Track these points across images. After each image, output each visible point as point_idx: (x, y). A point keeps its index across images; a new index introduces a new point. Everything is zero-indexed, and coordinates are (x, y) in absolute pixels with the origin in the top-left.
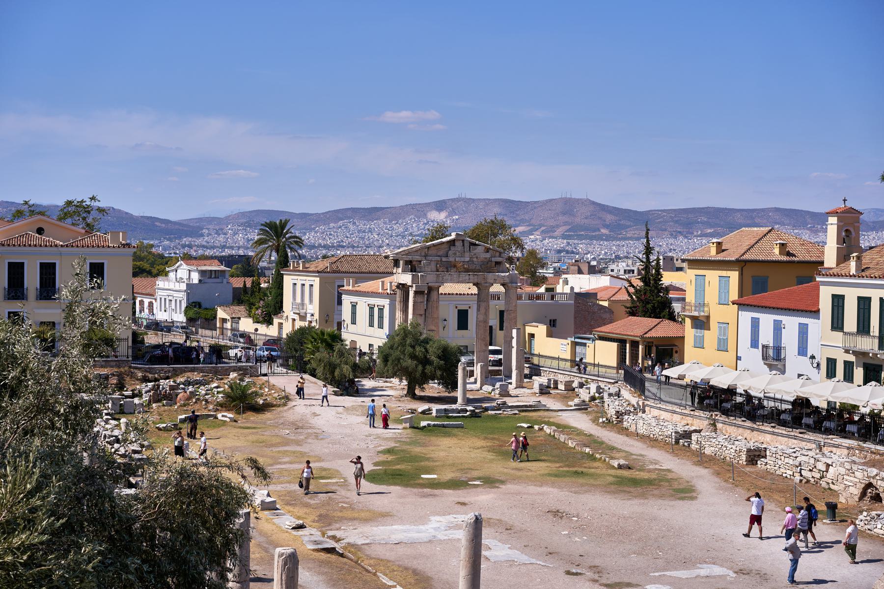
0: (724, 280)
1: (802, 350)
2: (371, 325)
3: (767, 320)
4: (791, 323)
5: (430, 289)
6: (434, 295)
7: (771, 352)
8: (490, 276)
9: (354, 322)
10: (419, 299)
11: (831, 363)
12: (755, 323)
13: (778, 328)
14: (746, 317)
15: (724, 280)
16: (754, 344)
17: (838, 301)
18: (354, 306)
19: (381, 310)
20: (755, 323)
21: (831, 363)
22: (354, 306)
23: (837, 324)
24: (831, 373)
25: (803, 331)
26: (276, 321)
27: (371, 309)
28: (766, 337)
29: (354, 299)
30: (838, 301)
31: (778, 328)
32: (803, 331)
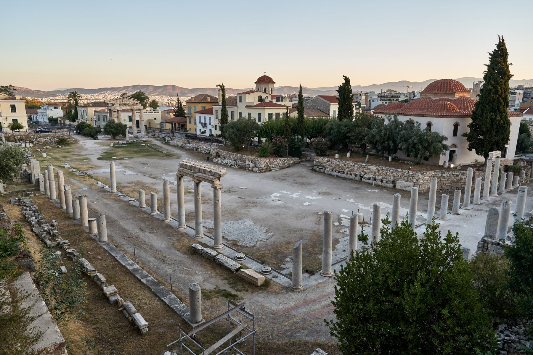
0: (195, 107)
1: (210, 124)
2: (104, 121)
3: (202, 116)
4: (208, 116)
5: (118, 111)
6: (120, 112)
7: (203, 125)
8: (135, 107)
9: (99, 120)
10: (115, 113)
11: (216, 126)
12: (200, 117)
13: (205, 118)
14: (198, 116)
15: (195, 107)
16: (200, 123)
17: (217, 111)
18: (99, 116)
19: (106, 117)
20: (200, 117)
21: (216, 126)
22: (99, 116)
23: (217, 117)
24: (216, 129)
25: (210, 118)
26: (76, 121)
27: (104, 116)
28: (202, 121)
29: (99, 114)
30: (217, 111)
31: (205, 118)
32: (210, 118)
